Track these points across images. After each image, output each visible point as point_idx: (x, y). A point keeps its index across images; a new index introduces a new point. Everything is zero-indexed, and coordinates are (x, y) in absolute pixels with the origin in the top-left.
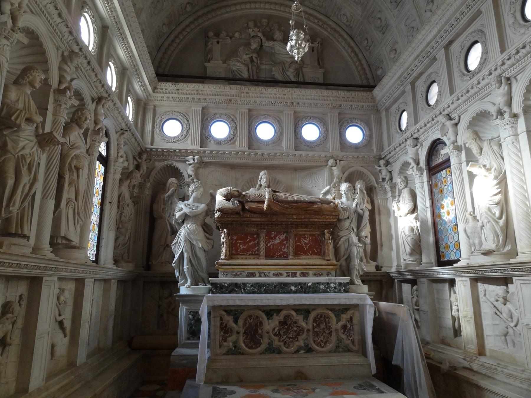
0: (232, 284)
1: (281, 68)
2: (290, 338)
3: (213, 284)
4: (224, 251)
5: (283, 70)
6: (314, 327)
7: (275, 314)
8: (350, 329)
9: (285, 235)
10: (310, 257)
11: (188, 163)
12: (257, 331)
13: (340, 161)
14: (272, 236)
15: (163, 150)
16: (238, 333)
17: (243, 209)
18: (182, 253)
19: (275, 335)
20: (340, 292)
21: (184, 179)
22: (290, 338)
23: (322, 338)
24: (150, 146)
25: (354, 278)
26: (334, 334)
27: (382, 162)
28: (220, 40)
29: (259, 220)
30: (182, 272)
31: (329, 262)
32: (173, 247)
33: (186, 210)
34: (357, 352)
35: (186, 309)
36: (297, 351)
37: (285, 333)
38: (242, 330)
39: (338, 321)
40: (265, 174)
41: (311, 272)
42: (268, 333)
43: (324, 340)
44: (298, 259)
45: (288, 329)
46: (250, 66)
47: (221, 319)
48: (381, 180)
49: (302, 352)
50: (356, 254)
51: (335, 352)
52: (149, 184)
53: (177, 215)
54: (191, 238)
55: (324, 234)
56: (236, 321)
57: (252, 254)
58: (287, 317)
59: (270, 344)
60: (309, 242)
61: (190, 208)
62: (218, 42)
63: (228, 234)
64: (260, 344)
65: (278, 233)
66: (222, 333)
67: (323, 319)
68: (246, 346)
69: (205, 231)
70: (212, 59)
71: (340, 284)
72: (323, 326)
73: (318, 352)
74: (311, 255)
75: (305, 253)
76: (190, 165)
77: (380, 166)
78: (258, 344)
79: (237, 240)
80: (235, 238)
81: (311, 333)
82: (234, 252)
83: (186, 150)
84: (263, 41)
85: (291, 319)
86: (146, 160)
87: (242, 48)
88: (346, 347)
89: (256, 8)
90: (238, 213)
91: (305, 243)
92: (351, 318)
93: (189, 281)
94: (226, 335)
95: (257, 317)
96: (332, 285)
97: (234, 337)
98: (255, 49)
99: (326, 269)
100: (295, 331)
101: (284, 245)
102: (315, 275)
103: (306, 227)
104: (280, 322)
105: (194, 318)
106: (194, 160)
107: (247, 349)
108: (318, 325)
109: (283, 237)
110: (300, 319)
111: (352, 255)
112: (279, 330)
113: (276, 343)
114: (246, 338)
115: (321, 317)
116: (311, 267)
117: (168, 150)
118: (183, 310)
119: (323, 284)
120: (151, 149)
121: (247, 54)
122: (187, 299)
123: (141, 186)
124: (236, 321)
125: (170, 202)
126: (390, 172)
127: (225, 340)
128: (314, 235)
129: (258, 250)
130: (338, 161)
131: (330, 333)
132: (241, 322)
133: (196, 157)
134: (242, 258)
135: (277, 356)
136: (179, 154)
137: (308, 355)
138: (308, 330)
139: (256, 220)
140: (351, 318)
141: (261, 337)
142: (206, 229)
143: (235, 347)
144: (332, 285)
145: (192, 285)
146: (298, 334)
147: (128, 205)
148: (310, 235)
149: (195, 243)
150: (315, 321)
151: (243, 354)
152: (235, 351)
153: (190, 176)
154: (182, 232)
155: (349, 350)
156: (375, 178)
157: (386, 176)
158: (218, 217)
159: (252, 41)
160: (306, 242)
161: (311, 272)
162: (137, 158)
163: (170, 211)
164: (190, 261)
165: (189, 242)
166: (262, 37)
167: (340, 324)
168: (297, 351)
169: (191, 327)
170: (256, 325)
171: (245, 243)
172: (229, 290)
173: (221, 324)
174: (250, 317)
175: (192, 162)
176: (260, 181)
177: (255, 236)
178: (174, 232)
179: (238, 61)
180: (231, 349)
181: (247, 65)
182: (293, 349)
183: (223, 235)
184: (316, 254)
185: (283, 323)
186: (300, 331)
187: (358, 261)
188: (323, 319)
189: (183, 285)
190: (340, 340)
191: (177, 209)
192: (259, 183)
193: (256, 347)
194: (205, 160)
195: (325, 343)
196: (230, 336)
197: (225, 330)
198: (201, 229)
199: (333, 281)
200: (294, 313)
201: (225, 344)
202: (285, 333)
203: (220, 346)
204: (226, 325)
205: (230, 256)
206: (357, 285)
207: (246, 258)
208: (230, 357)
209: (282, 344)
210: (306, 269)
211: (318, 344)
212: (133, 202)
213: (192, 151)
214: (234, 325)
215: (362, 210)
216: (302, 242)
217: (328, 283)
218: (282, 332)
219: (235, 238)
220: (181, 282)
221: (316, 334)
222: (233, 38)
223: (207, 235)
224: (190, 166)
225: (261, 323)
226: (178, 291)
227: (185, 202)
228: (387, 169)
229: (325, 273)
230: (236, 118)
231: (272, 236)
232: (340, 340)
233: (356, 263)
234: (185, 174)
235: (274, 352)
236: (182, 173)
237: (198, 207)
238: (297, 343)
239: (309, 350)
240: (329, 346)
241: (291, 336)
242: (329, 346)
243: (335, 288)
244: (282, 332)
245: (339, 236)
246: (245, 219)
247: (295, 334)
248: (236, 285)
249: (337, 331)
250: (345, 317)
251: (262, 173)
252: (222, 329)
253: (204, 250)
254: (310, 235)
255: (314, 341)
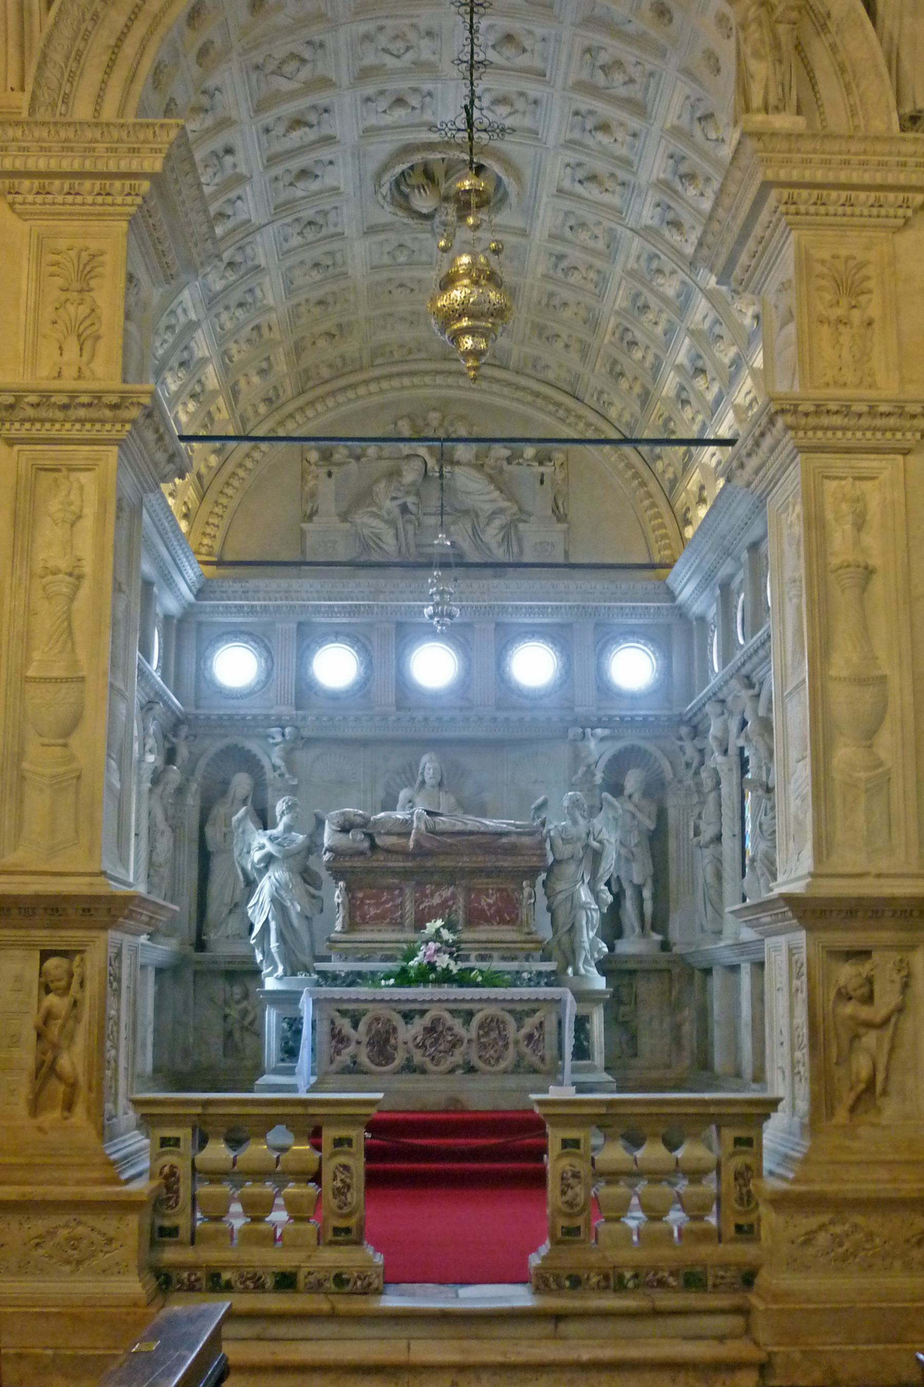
0: (352, 972)
1: (469, 526)
2: (440, 1052)
3: (320, 973)
4: (341, 919)
5: (474, 528)
6: (479, 1037)
7: (417, 1017)
8: (538, 1040)
9: (451, 889)
10: (496, 927)
11: (271, 741)
12: (387, 1040)
13: (593, 728)
14: (428, 892)
15: (220, 717)
16: (359, 1043)
17: (374, 847)
18: (267, 922)
19: (417, 1046)
20: (538, 984)
21: (264, 774)
22: (440, 1052)
23: (492, 1052)
24: (191, 710)
25: (581, 965)
26: (511, 1046)
27: (684, 730)
28: (334, 470)
29: (401, 864)
30: (267, 954)
31: (529, 937)
32: (250, 912)
33: (270, 848)
34: (548, 1073)
35: (278, 1015)
36: (452, 1071)
37: (432, 1045)
38: (365, 1039)
39: (519, 1028)
40: (431, 761)
41: (495, 954)
42: (405, 1043)
43: (495, 1056)
44: (474, 931)
45: (437, 1039)
46: (400, 526)
47: (333, 1022)
48: (683, 766)
49: (460, 1071)
50: (584, 922)
51: (513, 1072)
52: (195, 785)
53: (257, 856)
54: (281, 896)
55: (522, 889)
56: (355, 1026)
57: (390, 923)
58: (436, 1021)
59: (409, 1060)
60: (495, 903)
61: (279, 844)
62: (330, 474)
63: (348, 889)
64: (394, 1059)
65: (439, 885)
66: (334, 1043)
67: (494, 1024)
68: (372, 1062)
69: (305, 881)
70: (317, 511)
71: (540, 974)
72: (494, 1035)
73: (484, 1073)
74: (498, 924)
75: (488, 920)
76: (276, 744)
77: (680, 739)
78: (389, 1059)
79: (362, 900)
80: (360, 895)
81: (474, 1045)
82: (358, 919)
83: (267, 717)
84: (429, 466)
85: (444, 1024)
86: (187, 738)
87: (383, 485)
88: (531, 1066)
89: (414, 386)
90: (362, 853)
91: (489, 905)
92: (541, 1023)
93: (281, 968)
94: (340, 1046)
95: (389, 1020)
96: (526, 975)
97: (351, 1049)
98: (413, 484)
99: (522, 949)
100: (450, 1042)
101: (451, 907)
102: (504, 959)
103: (488, 877)
104: (425, 1029)
105: (290, 1028)
106: (283, 735)
107: (373, 1067)
108: (487, 1034)
109: (447, 893)
110: (457, 1024)
111: (577, 925)
112: (424, 1040)
113: (418, 1058)
114: (371, 1051)
115: (492, 1021)
116: (495, 945)
117: (231, 717)
118: (271, 1017)
119: (509, 973)
120: (197, 717)
121: (394, 498)
122: (276, 998)
123: (180, 791)
124: (355, 1026)
125: (240, 830)
126: (701, 751)
127: (338, 1053)
128: (505, 890)
129: (402, 917)
130: (589, 730)
131: (506, 1046)
132: (362, 1027)
133: (287, 730)
134: (372, 931)
135: (422, 1077)
136: (252, 724)
137: (467, 1076)
138: (470, 1041)
139: (396, 864)
140: (541, 1023)
141: (396, 1049)
142: (307, 877)
143: (355, 1063)
144: (526, 975)
145: (285, 975)
146: (454, 1046)
147: (163, 833)
148: (498, 890)
149: (288, 904)
150: (481, 1027)
151: (366, 1073)
152: (353, 1068)
153: (275, 768)
154: (266, 887)
155: (535, 1071)
156: (671, 763)
157: (692, 759)
158: (328, 861)
159: (405, 467)
160: (491, 901)
161: (495, 954)
162: (170, 736)
163: (240, 845)
164: (281, 937)
165: (277, 902)
166: (428, 458)
167: (524, 1031)
168: (452, 1071)
169: (286, 1043)
170: (387, 1032)
171: (378, 905)
172: (348, 981)
173: (333, 1029)
174: (377, 1019)
175: (279, 739)
176: (422, 774)
177: (397, 892)
178: (251, 885)
179: (374, 515)
180: (348, 1066)
181: (392, 523)
182: (445, 1066)
183: (337, 892)
184: (508, 923)
185: (430, 1030)
186: (456, 1043)
187: (592, 934)
188: (494, 1024)
189: (270, 974)
190: (520, 1056)
191: (255, 845)
192: (420, 778)
193: (387, 1064)
194: (305, 733)
195: (497, 1060)
196: (346, 1047)
197: (338, 1038)
198: (299, 879)
199: (527, 968)
200: (447, 1015)
201: (338, 1058)
202: (432, 1045)
203: (332, 1062)
204: (340, 1031)
205: (351, 925)
206: (582, 976)
207: (380, 931)
208: (347, 1076)
209: (427, 1059)
210: (486, 949)
211: (487, 1062)
212: (171, 826)
213: (279, 718)
214: (352, 1031)
215: (600, 842)
216: (483, 903)
217: (517, 972)
218: (428, 1043)
219: (360, 895)
220: (266, 971)
221: (483, 1047)
222: (363, 459)
223: (312, 890)
224: (277, 749)
225: (395, 1029)
226: (262, 984)
227: (268, 832)
228: (695, 746)
229: (522, 955)
230: (370, 642)
231: (428, 892)
232: (520, 1056)
233: (585, 938)
234: (266, 762)
235: (414, 1071)
236: (259, 760)
237: (292, 841)
238: (452, 1059)
239: (471, 1070)
240: (502, 1065)
241: (442, 1048)
242: (502, 1065)
243: (530, 979)
244: (428, 1043)
245: (554, 889)
246: (375, 864)
247: (448, 1045)
248: (359, 974)
249: (517, 1043)
250: (530, 1023)
251: (425, 758)
252: (333, 1037)
253: (307, 917)
254: (498, 890)
255: (480, 1057)
